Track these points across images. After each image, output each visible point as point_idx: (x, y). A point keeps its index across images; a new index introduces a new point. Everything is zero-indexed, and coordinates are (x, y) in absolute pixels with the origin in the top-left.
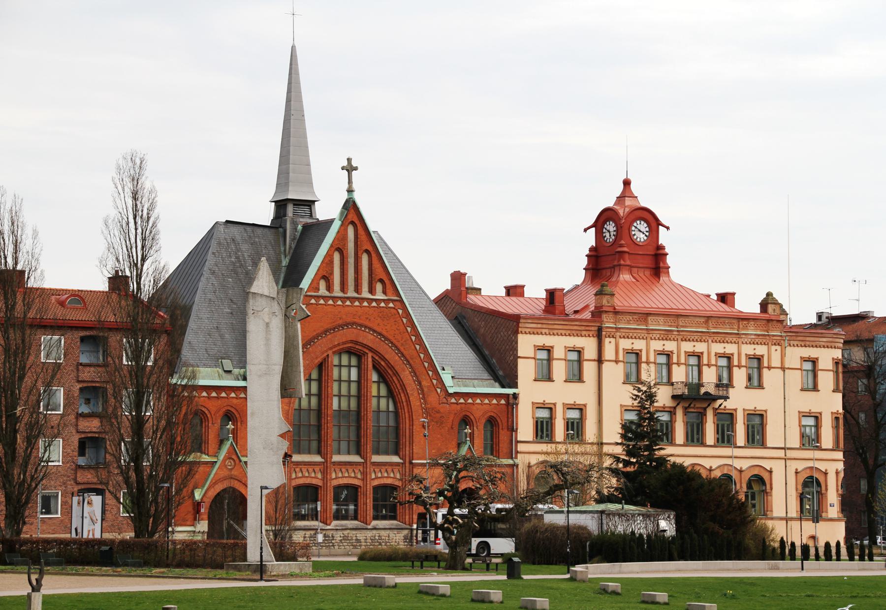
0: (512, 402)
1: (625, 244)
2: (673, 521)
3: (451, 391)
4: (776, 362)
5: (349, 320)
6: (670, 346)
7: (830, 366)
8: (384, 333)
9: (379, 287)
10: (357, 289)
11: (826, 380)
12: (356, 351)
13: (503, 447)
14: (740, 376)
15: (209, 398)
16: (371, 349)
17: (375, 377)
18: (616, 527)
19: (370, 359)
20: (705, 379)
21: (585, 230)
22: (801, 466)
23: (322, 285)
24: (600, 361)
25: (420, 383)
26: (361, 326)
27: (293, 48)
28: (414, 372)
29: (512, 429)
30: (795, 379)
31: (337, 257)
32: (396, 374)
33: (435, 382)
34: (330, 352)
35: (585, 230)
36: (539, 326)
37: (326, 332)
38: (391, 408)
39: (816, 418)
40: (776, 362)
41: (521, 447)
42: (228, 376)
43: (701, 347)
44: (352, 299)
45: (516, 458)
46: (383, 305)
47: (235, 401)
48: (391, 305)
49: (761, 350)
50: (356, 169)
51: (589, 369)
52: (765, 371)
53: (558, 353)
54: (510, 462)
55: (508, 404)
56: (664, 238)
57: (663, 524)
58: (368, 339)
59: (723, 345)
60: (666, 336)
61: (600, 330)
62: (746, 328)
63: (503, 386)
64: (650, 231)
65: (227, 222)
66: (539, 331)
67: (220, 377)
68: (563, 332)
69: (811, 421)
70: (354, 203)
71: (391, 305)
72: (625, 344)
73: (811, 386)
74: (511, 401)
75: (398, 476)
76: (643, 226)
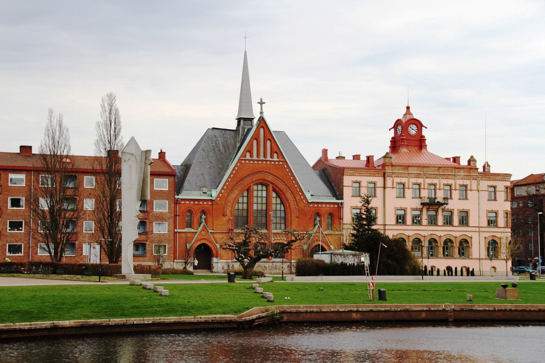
0: (340, 206)
1: (408, 135)
2: (368, 258)
3: (310, 201)
4: (474, 187)
5: (260, 170)
6: (420, 181)
7: (503, 189)
8: (278, 175)
9: (275, 155)
10: (265, 156)
11: (501, 196)
12: (264, 183)
14: (456, 194)
15: (194, 204)
16: (271, 183)
17: (274, 195)
18: (338, 260)
19: (271, 187)
20: (437, 196)
21: (390, 130)
22: (487, 235)
23: (248, 154)
24: (384, 188)
25: (295, 198)
26: (266, 172)
27: (245, 52)
28: (292, 193)
29: (341, 218)
30: (485, 195)
31: (255, 142)
32: (284, 194)
33: (302, 197)
34: (252, 184)
35: (390, 130)
37: (249, 175)
38: (282, 209)
39: (496, 213)
40: (474, 187)
41: (345, 226)
42: (205, 195)
43: (435, 181)
44: (262, 161)
46: (277, 163)
47: (206, 206)
48: (281, 163)
49: (466, 182)
50: (264, 103)
52: (469, 192)
53: (364, 184)
54: (340, 233)
55: (338, 207)
56: (425, 132)
57: (363, 259)
58: (270, 178)
59: (447, 180)
60: (418, 176)
61: (384, 174)
62: (459, 172)
63: (338, 199)
64: (418, 129)
65: (213, 128)
67: (201, 195)
69: (494, 215)
70: (263, 118)
71: (281, 163)
73: (493, 198)
74: (340, 206)
75: (285, 239)
76: (414, 127)
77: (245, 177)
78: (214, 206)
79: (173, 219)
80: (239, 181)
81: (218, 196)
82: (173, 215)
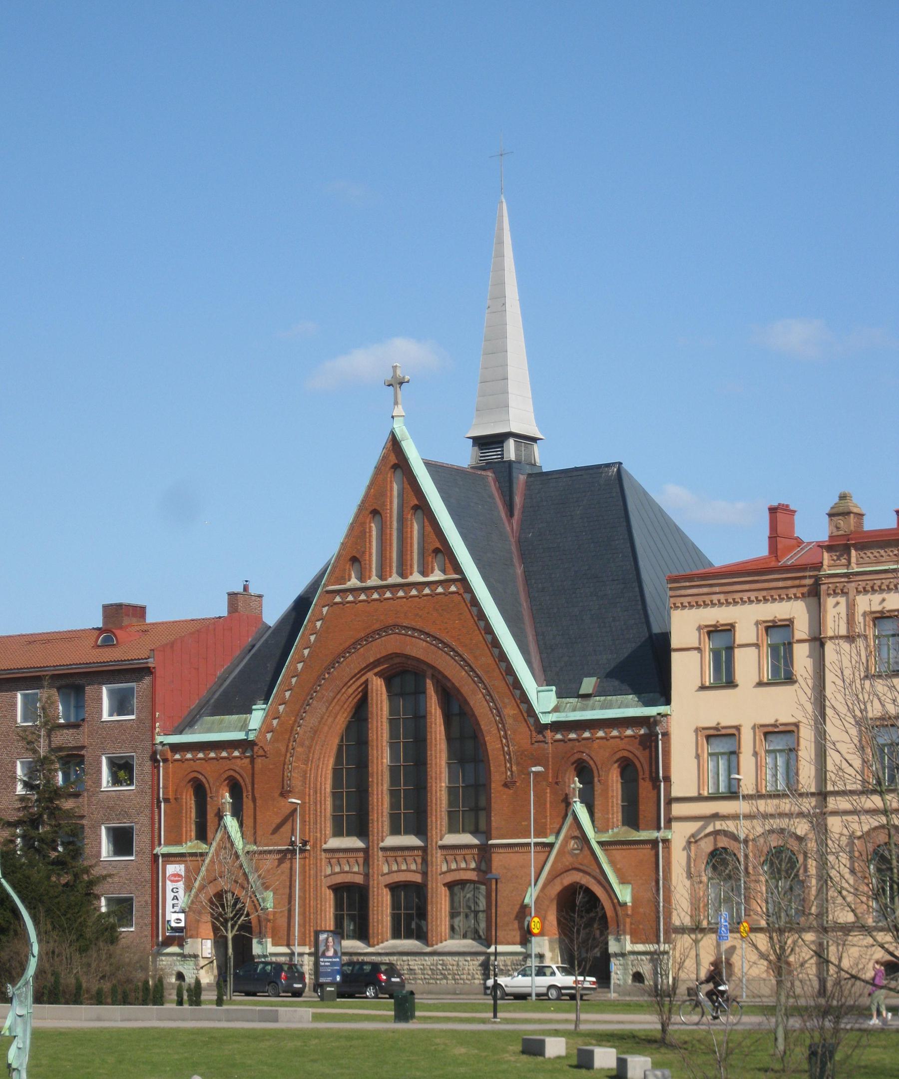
3: (545, 720)
13: (645, 809)
24: (818, 641)
36: (705, 590)
44: (394, 587)
45: (668, 826)
51: (802, 655)
53: (745, 633)
58: (418, 648)
66: (707, 599)
68: (753, 596)
72: (866, 603)
77: (342, 654)
78: (259, 762)
79: (147, 812)
80: (327, 669)
81: (266, 727)
82: (148, 799)
